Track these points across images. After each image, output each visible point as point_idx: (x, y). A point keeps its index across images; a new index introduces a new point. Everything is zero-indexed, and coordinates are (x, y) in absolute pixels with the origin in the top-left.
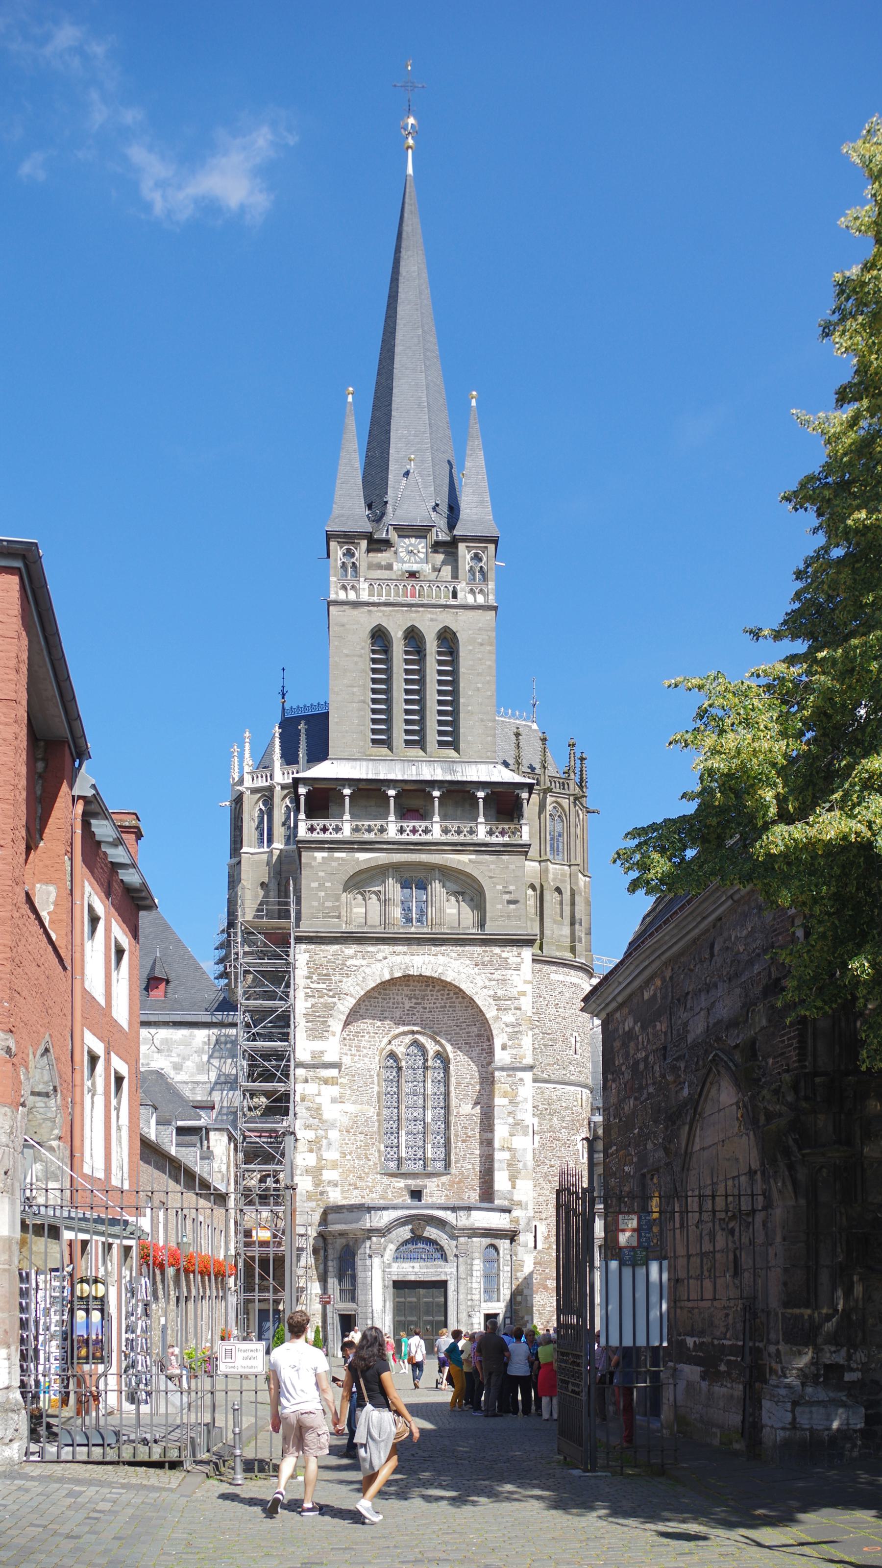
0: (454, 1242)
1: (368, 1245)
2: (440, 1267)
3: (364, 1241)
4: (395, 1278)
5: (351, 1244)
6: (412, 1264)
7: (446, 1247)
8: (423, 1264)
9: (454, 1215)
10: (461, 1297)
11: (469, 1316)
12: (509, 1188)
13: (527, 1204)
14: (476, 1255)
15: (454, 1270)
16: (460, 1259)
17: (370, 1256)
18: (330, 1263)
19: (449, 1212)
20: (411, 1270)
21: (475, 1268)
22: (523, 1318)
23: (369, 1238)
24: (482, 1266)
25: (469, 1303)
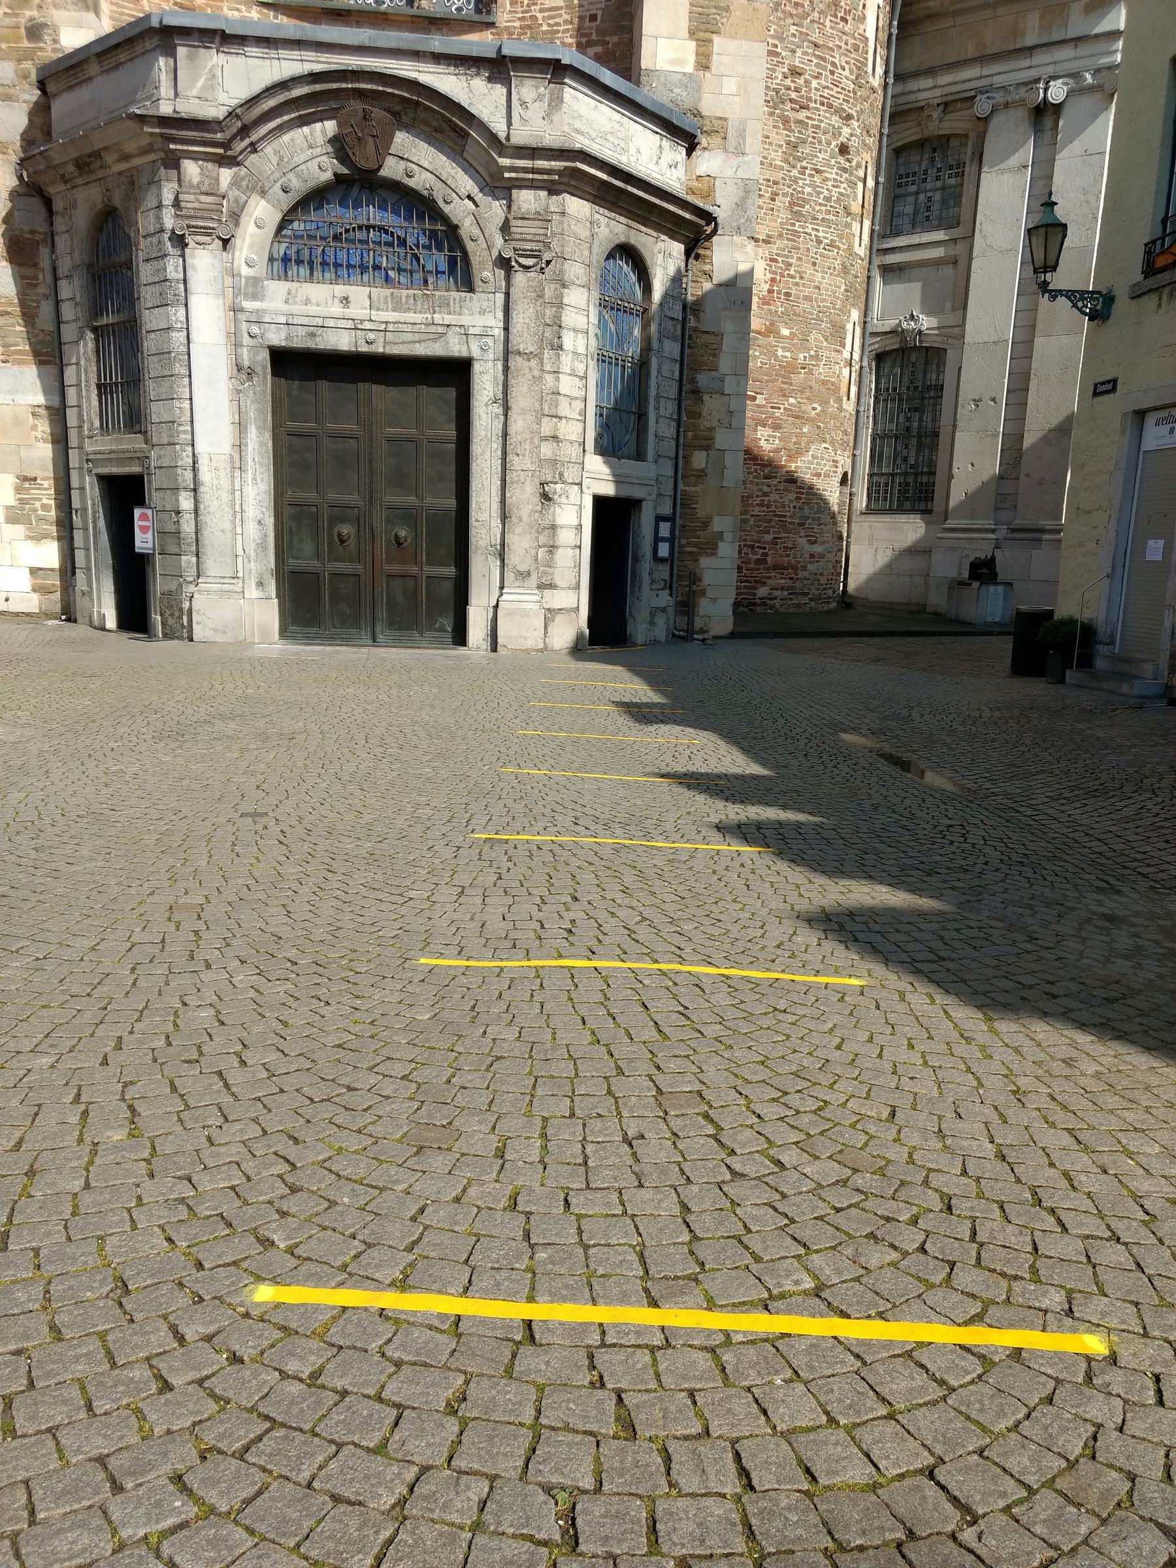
0: (495, 210)
1: (168, 197)
2: (445, 305)
3: (154, 182)
4: (277, 338)
5: (117, 202)
6: (340, 289)
7: (467, 228)
8: (381, 293)
9: (500, 90)
10: (518, 424)
11: (546, 497)
12: (689, 68)
13: (742, 134)
14: (574, 271)
15: (495, 322)
16: (520, 279)
17: (180, 242)
18: (66, 290)
19: (479, 84)
20: (337, 309)
21: (571, 318)
22: (706, 523)
23: (173, 162)
24: (594, 319)
25: (547, 450)
